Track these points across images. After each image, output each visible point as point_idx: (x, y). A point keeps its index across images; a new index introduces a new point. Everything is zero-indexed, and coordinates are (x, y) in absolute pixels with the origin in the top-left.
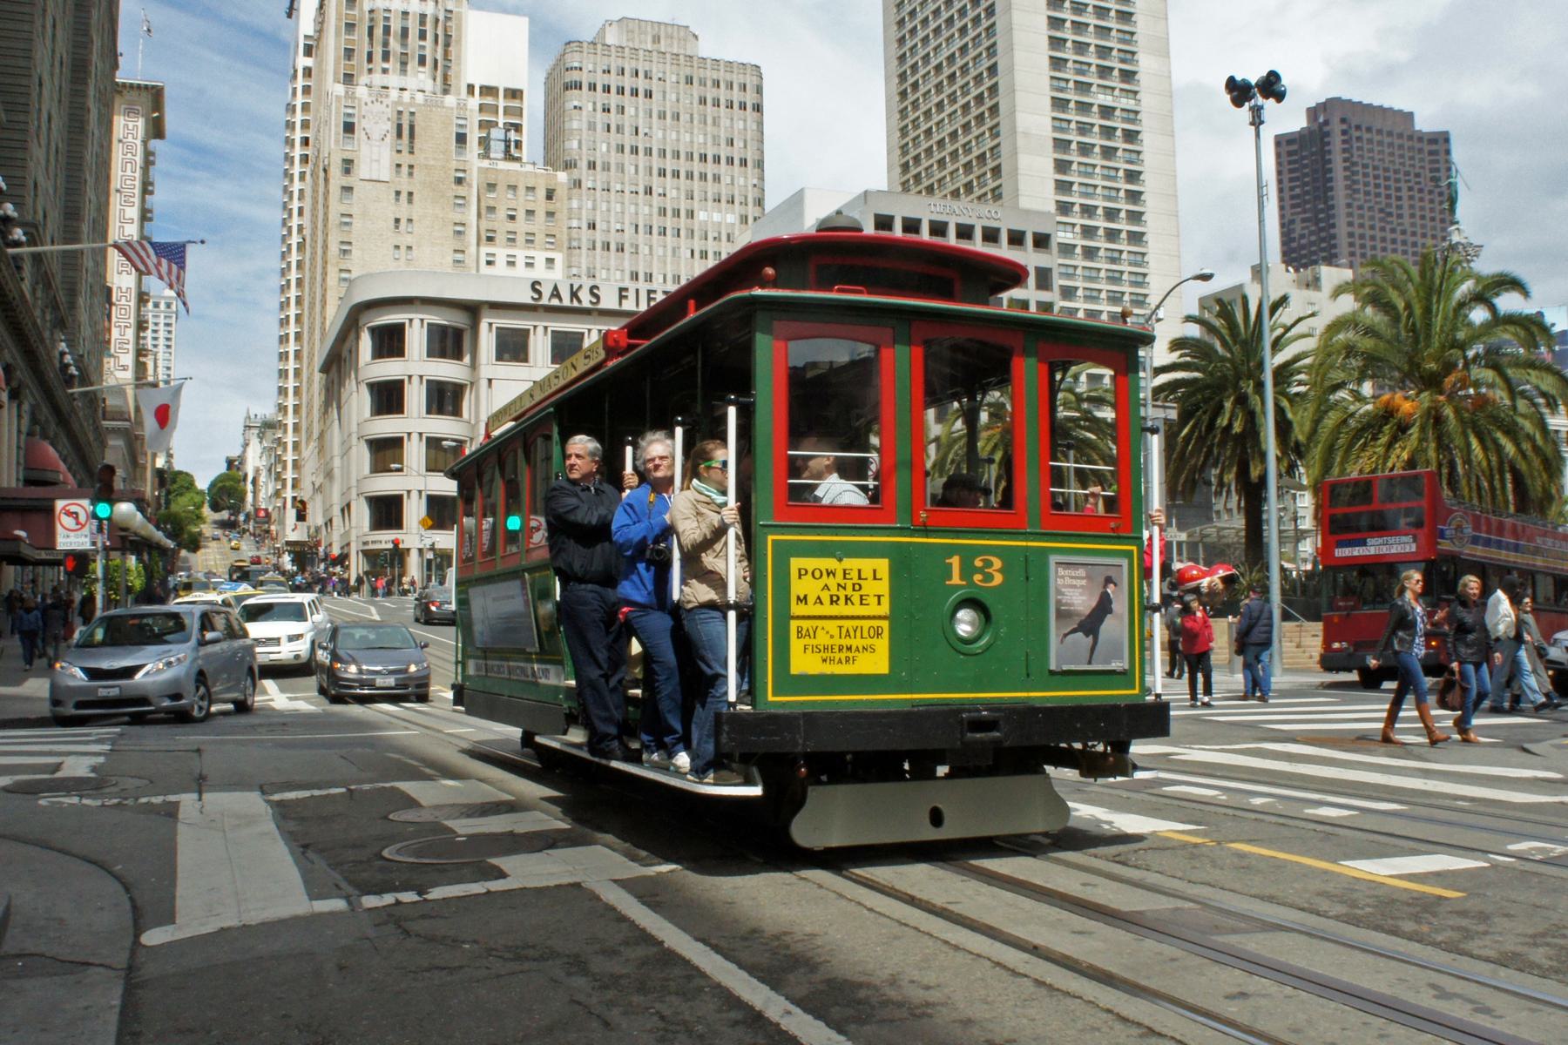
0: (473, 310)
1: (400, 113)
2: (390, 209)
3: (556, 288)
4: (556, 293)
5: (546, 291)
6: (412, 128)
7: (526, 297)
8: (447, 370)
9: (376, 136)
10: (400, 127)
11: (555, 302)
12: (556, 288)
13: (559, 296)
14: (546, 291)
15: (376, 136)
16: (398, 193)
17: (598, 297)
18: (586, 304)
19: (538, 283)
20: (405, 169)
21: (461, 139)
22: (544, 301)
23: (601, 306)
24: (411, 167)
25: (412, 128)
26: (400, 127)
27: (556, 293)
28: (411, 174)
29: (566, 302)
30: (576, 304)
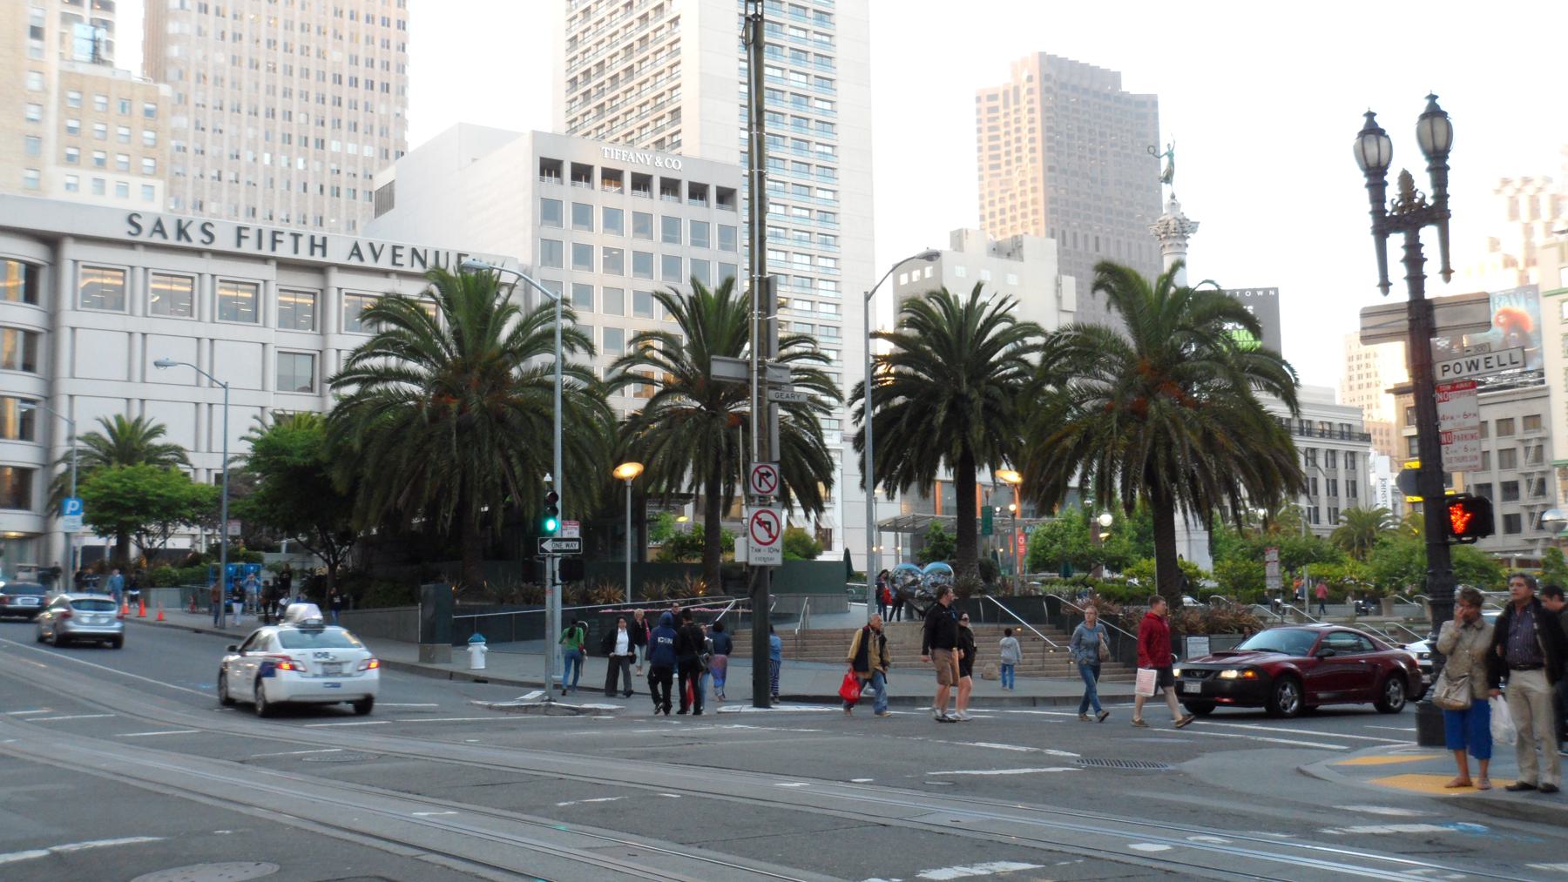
0: (52, 241)
4: (159, 228)
5: (147, 224)
7: (121, 231)
11: (157, 239)
12: (159, 223)
13: (163, 232)
14: (147, 224)
18: (196, 244)
19: (138, 216)
22: (143, 237)
23: (212, 247)
27: (159, 228)
29: (172, 240)
30: (183, 243)
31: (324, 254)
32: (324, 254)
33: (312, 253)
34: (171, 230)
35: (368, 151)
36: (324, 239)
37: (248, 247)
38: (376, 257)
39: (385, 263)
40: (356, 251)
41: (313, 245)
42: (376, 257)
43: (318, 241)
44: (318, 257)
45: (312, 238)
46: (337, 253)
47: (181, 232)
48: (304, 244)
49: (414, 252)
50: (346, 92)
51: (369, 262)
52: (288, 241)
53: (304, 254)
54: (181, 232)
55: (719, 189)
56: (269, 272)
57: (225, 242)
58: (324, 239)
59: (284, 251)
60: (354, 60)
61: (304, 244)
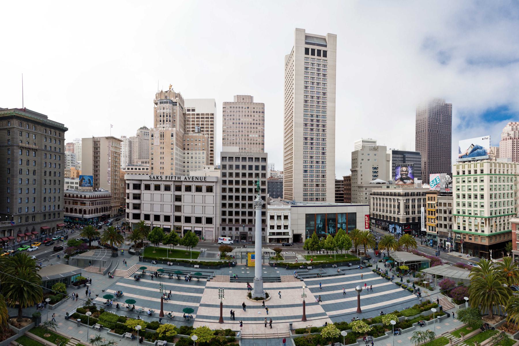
8: (137, 192)
14: (152, 177)
34: (156, 178)
35: (257, 136)
37: (168, 179)
39: (191, 180)
40: (186, 178)
46: (183, 179)
47: (157, 178)
48: (177, 178)
50: (252, 126)
51: (188, 180)
52: (174, 178)
53: (177, 180)
54: (157, 178)
56: (172, 183)
57: (164, 179)
59: (174, 179)
60: (254, 120)
61: (177, 178)
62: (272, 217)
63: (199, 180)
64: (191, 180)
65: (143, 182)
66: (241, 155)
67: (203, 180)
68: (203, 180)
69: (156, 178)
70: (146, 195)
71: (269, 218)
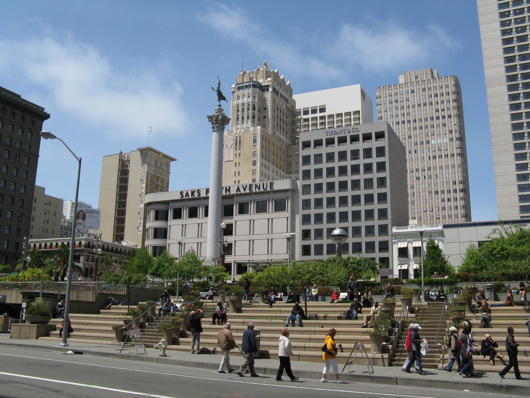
1: (237, 137)
2: (234, 169)
3: (187, 192)
4: (187, 194)
6: (240, 141)
7: (178, 197)
9: (229, 146)
10: (236, 141)
12: (187, 192)
14: (184, 194)
15: (229, 146)
16: (236, 164)
17: (200, 194)
18: (196, 196)
20: (238, 155)
21: (255, 141)
24: (240, 154)
25: (240, 141)
26: (236, 141)
27: (187, 194)
28: (239, 156)
29: (190, 197)
31: (229, 192)
32: (229, 192)
33: (226, 192)
34: (190, 194)
36: (229, 187)
38: (245, 190)
39: (247, 191)
40: (238, 189)
41: (226, 190)
42: (245, 190)
43: (228, 188)
44: (228, 193)
45: (226, 188)
47: (193, 193)
49: (256, 185)
51: (242, 191)
54: (193, 193)
55: (376, 133)
58: (229, 187)
62: (403, 252)
63: (262, 190)
64: (247, 191)
65: (171, 205)
66: (336, 133)
67: (269, 189)
68: (269, 189)
69: (190, 194)
70: (174, 226)
71: (396, 253)
